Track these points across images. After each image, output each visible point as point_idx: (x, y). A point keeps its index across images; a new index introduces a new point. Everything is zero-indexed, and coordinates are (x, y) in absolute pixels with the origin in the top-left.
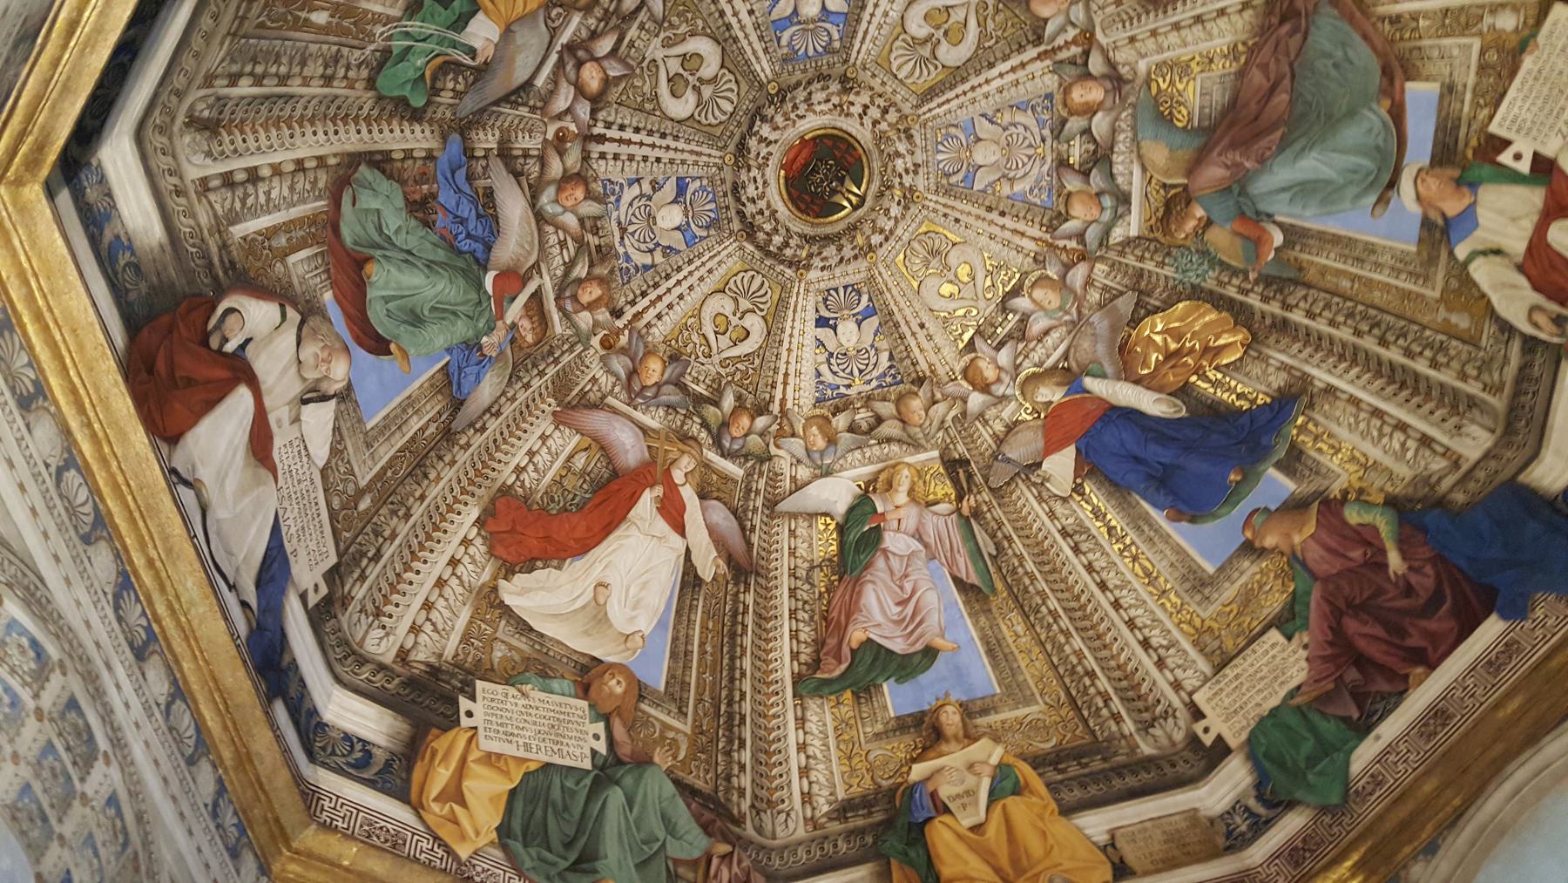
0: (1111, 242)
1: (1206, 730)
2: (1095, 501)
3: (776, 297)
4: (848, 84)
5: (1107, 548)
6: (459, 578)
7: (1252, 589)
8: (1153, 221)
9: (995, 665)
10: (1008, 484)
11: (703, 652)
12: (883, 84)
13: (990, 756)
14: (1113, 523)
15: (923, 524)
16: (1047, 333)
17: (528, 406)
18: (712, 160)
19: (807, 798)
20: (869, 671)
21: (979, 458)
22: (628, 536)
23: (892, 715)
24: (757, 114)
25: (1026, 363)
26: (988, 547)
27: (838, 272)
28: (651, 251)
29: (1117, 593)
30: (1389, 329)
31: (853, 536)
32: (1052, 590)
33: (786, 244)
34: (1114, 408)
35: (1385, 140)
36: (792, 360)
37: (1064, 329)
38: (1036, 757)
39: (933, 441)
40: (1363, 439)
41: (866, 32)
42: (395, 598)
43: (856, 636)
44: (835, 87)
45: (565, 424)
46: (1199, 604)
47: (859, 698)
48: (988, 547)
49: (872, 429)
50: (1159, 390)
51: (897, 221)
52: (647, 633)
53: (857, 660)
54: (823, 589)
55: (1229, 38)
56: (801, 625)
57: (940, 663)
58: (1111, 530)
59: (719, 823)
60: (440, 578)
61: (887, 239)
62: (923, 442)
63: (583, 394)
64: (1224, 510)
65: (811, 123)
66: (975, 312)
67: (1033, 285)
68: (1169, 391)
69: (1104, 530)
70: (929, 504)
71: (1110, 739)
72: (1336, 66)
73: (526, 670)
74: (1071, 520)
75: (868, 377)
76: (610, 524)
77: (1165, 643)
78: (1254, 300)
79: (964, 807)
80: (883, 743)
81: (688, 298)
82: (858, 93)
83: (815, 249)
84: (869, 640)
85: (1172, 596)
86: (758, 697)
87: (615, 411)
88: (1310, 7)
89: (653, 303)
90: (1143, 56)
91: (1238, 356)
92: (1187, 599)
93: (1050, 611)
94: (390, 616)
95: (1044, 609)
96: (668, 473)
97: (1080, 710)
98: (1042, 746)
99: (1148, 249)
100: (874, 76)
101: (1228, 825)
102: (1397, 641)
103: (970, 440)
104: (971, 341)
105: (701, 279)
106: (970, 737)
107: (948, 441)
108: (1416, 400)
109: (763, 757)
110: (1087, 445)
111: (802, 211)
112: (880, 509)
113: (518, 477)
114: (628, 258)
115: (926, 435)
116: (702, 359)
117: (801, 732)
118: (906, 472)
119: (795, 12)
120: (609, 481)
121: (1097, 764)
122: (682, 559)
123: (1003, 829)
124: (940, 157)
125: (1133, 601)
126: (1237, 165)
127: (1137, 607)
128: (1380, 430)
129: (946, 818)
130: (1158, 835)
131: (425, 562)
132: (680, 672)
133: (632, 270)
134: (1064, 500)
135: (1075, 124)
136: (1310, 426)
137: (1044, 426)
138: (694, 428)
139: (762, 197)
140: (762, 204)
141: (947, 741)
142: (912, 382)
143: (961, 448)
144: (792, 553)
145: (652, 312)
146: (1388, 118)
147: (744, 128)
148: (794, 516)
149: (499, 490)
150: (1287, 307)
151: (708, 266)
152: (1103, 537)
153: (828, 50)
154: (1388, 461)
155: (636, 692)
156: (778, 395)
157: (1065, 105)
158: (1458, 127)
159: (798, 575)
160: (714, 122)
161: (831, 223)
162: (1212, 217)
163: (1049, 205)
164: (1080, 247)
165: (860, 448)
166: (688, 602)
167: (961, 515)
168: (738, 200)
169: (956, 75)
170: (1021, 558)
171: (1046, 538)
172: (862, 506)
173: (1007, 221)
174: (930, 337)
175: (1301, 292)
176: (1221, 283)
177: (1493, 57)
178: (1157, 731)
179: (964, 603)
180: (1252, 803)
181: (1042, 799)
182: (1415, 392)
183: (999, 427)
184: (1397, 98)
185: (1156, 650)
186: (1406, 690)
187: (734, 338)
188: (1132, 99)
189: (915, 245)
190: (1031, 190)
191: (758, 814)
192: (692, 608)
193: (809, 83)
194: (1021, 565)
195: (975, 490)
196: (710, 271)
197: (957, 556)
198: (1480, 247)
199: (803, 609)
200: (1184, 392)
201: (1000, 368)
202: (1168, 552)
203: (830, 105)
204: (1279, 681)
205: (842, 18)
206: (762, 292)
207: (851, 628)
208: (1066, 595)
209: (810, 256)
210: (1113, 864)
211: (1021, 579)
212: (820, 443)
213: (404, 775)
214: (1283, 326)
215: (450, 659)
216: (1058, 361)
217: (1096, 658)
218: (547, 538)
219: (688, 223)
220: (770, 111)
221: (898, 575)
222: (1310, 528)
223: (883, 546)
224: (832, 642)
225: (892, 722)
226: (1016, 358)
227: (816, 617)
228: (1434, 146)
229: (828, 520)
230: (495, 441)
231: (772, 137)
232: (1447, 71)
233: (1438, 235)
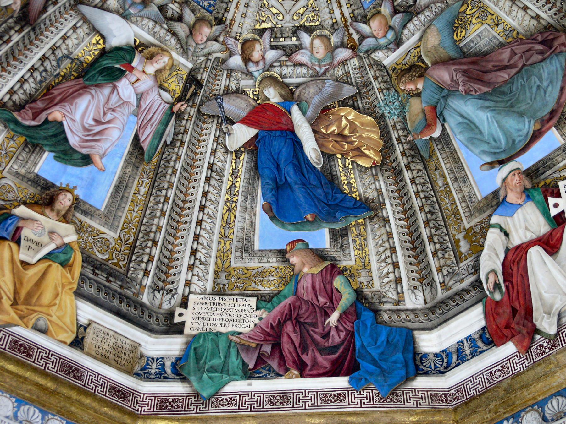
0: (372, 56)
1: (181, 315)
2: (240, 166)
5: (223, 193)
7: (265, 273)
8: (398, 67)
9: (113, 197)
10: (209, 117)
13: (66, 236)
14: (237, 184)
15: (148, 94)
16: (301, 65)
20: (46, 138)
21: (208, 91)
23: (36, 171)
25: (277, 70)
26: (168, 137)
29: (205, 217)
31: (106, 63)
32: (177, 187)
34: (293, 132)
35: (520, 141)
37: (311, 72)
38: (89, 257)
39: (195, 58)
40: (376, 255)
43: (56, 114)
47: (26, 146)
48: (168, 137)
49: (172, 19)
50: (320, 145)
53: (45, 126)
54: (62, 74)
56: (31, 80)
57: (86, 170)
58: (233, 186)
62: (190, 53)
64: (290, 227)
66: (280, 18)
67: (318, 36)
68: (324, 151)
69: (230, 183)
70: (161, 87)
71: (132, 279)
74: (220, 164)
78: (399, 149)
80: (17, 181)
84: (61, 123)
85: (228, 242)
91: (367, 166)
92: (233, 250)
93: (166, 196)
95: (164, 192)
97: (133, 254)
98: (97, 254)
99: (383, 76)
101: (148, 364)
102: (300, 353)
103: (214, 77)
104: (263, 31)
106: (65, 218)
107: (203, 66)
108: (413, 260)
110: (262, 137)
112: (134, 64)
115: (195, 52)
118: (166, 59)
121: (115, 285)
123: (40, 274)
125: (208, 228)
127: (207, 232)
128: (386, 258)
129: (14, 246)
130: (111, 342)
134: (227, 151)
136: (362, 227)
137: (254, 107)
141: (52, 210)
142: (216, 18)
143: (205, 76)
144: (65, 38)
146: (531, 133)
148: (85, 19)
150: (408, 167)
152: (225, 187)
154: (375, 274)
158: (550, 168)
159: (56, 52)
162: (422, 95)
164: (357, 42)
165: (156, 22)
167: (171, 108)
170: (179, 157)
171: (200, 160)
176: (394, 127)
179: (129, 152)
180: (168, 364)
181: (73, 279)
182: (416, 257)
183: (233, 86)
184: (544, 129)
185: (195, 259)
186: (282, 376)
194: (175, 162)
195: (190, 104)
197: (149, 126)
198: (503, 226)
199: (41, 73)
200: (328, 157)
201: (263, 58)
202: (247, 221)
204: (235, 323)
207: (57, 107)
210: (77, 337)
211: (168, 167)
214: (397, 172)
216: (292, 84)
217: (165, 237)
221: (110, 106)
222: (316, 270)
223: (117, 84)
224: (40, 105)
225: (32, 175)
226: (276, 61)
228: (534, 165)
229: (101, 41)
233: (494, 203)
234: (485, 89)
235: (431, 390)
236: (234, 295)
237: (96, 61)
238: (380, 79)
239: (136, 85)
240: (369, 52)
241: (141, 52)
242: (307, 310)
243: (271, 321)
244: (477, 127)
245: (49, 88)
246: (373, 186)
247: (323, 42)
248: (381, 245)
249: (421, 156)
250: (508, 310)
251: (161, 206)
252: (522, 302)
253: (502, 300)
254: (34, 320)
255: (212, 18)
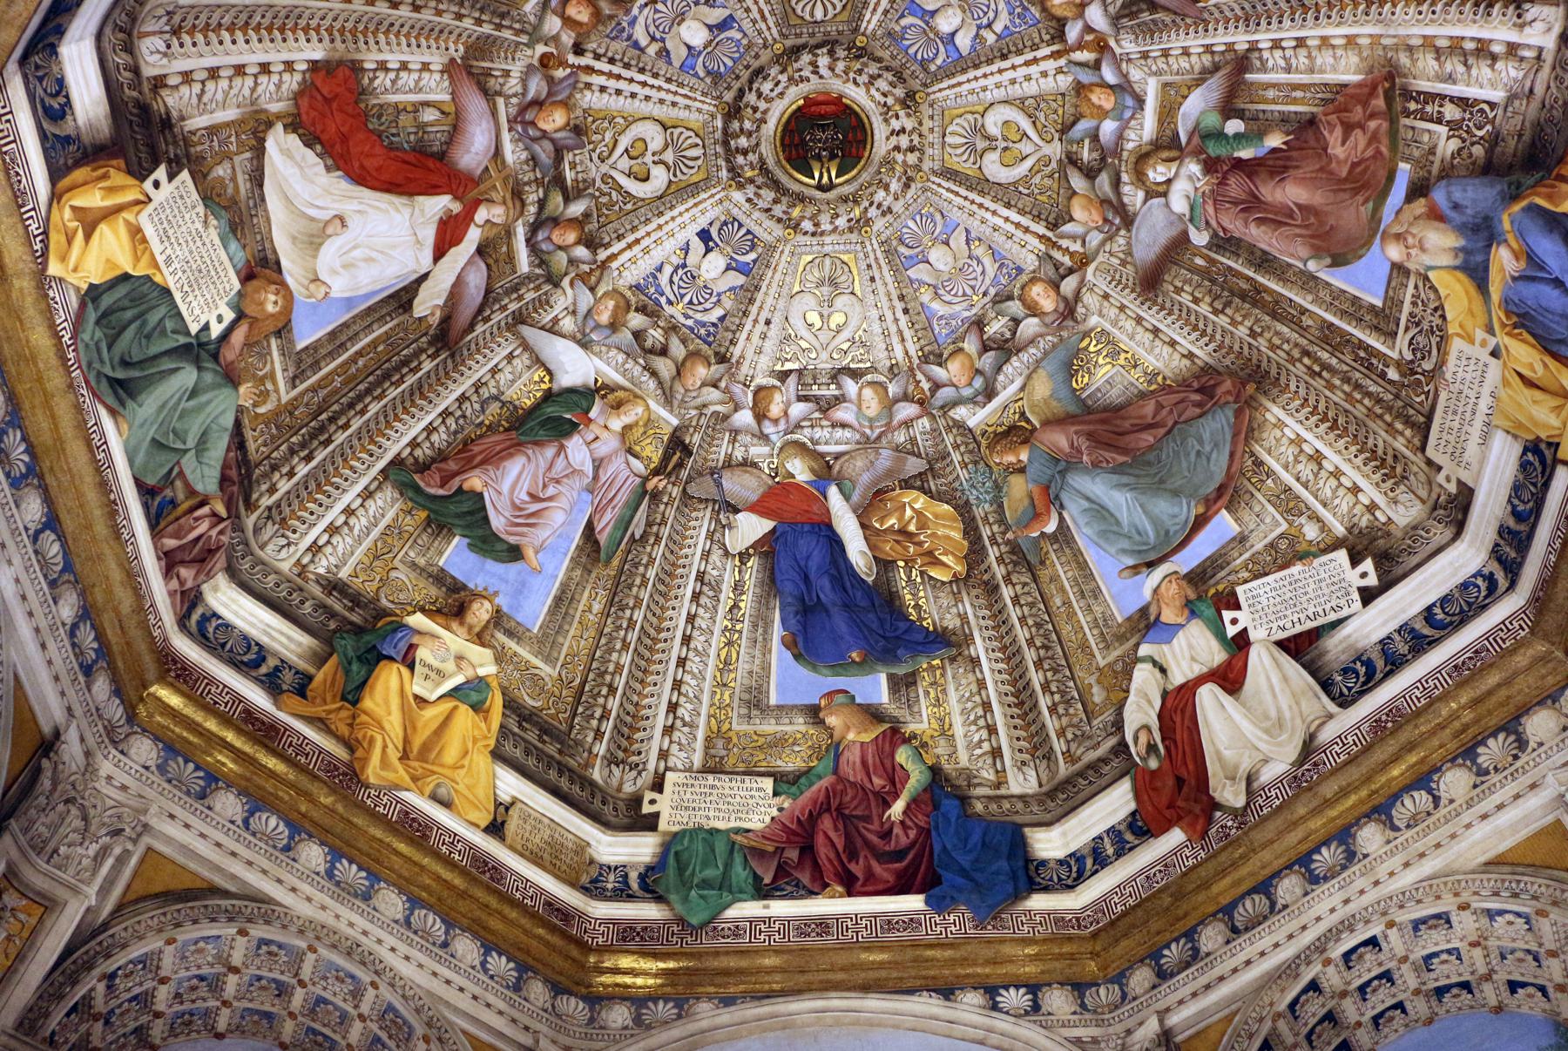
0: (951, 413)
1: (652, 802)
3: (695, 179)
4: (909, 101)
6: (256, 83)
8: (990, 430)
10: (700, 500)
11: (353, 360)
12: (932, 130)
14: (742, 605)
16: (844, 426)
17: (441, 31)
18: (767, 34)
19: (315, 549)
20: (459, 516)
22: (398, 210)
24: (830, 44)
25: (807, 431)
26: (637, 527)
27: (756, 215)
28: (653, 39)
29: (691, 654)
30: (1052, 658)
31: (551, 410)
33: (745, 153)
34: (829, 526)
35: (1176, 532)
36: (654, 236)
37: (858, 436)
41: (960, 84)
42: (200, 38)
43: (475, 481)
44: (900, 92)
45: (451, 76)
46: (739, 716)
48: (637, 527)
49: (651, 351)
50: (872, 547)
51: (835, 230)
52: (333, 294)
55: (1160, 365)
56: (442, 429)
58: (735, 606)
59: (235, 489)
60: (244, 66)
61: (813, 234)
62: (676, 403)
63: (488, 73)
64: (825, 671)
65: (857, 95)
66: (813, 355)
67: (871, 384)
69: (731, 603)
70: (630, 451)
72: (1198, 453)
73: (225, 208)
74: (715, 573)
75: (691, 313)
76: (398, 185)
77: (687, 719)
78: (993, 553)
79: (427, 677)
80: (413, 575)
81: (637, 102)
82: (909, 115)
83: (760, 180)
84: (480, 496)
85: (727, 694)
86: (355, 442)
87: (494, 113)
88: (1223, 400)
89: (610, 75)
90: (1101, 315)
92: (735, 705)
94: (182, 45)
95: (628, 612)
96: (477, 203)
99: (967, 444)
100: (932, 117)
103: (710, 441)
105: (662, 101)
106: (480, 638)
108: (1018, 721)
109: (312, 486)
111: (782, 144)
112: (592, 414)
113: (375, 70)
114: (633, 23)
116: (595, 156)
117: (359, 501)
118: (640, 410)
119: (933, 13)
120: (432, 155)
121: (552, 749)
122: (415, 276)
123: (441, 719)
124: (911, 224)
126: (1080, 452)
127: (694, 676)
129: (405, 671)
131: (247, 42)
132: (323, 352)
133: (625, 35)
134: (727, 553)
135: (1015, 307)
138: (532, 197)
139: (769, 100)
140: (762, 105)
141: (462, 624)
142: (716, 354)
143: (696, 439)
144: (494, 371)
145: (601, 80)
147: (812, 42)
148: (526, 346)
149: (353, 62)
150: (1008, 579)
151: (678, 99)
153: (924, 64)
155: (280, 325)
156: (615, 249)
157: (1023, 288)
160: (799, 11)
161: (791, 176)
163: (941, 341)
166: (384, 311)
167: (643, 484)
168: (751, 82)
169: (981, 184)
170: (652, 561)
172: (582, 397)
173: (903, 320)
174: (764, 337)
175: (1026, 578)
176: (986, 519)
177: (1283, 545)
178: (616, 771)
180: (633, 876)
182: (1023, 716)
183: (739, 454)
187: (634, 169)
188: (1065, 334)
189: (828, 261)
190: (941, 318)
191: (268, 518)
192: (381, 320)
193: (887, 69)
194: (646, 567)
196: (674, 104)
200: (885, 565)
201: (786, 413)
202: (757, 662)
203: (882, 100)
205: (956, 56)
206: (690, 163)
208: (654, 620)
209: (751, 181)
212: (604, 318)
213: (70, 162)
214: (991, 589)
215: (186, 129)
218: (345, 139)
219: (700, 53)
220: (841, 53)
221: (553, 474)
223: (565, 443)
224: (452, 465)
226: (804, 419)
227: (460, 436)
229: (547, 379)
230: (392, 25)
231: (824, 71)
232: (1252, 526)
233: (1142, 626)
234: (1121, 459)
235: (1055, 911)
236: (737, 773)
237: (537, 407)
238: (962, 449)
239: (594, 445)
240: (947, 407)
241: (604, 397)
242: (853, 798)
243: (797, 813)
244: (1112, 515)
245: (467, 443)
246: (954, 610)
247: (876, 392)
248: (968, 700)
249: (1028, 563)
250: (1170, 782)
251: (622, 633)
252: (1191, 767)
253: (1160, 768)
254: (431, 786)
255: (710, 352)
